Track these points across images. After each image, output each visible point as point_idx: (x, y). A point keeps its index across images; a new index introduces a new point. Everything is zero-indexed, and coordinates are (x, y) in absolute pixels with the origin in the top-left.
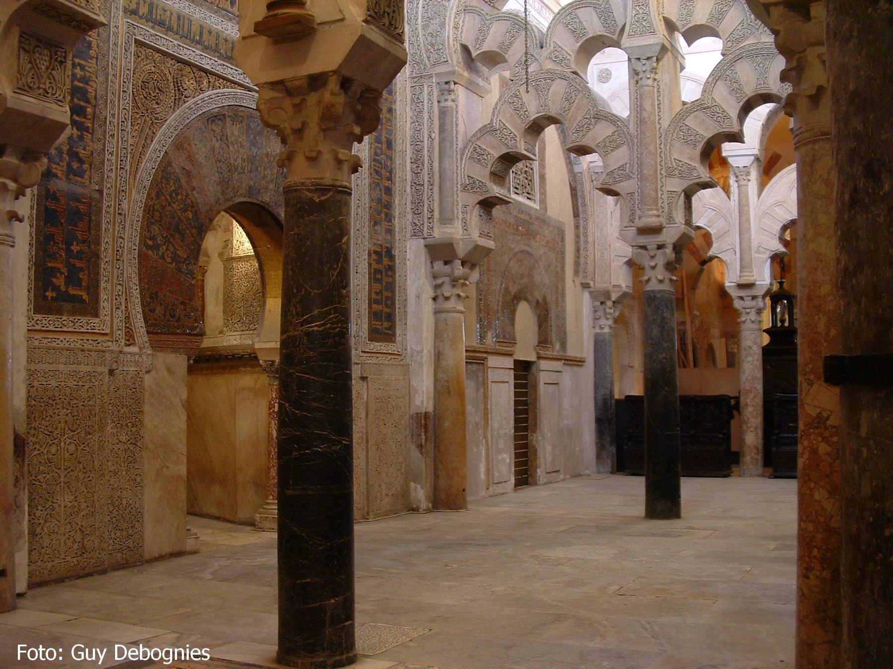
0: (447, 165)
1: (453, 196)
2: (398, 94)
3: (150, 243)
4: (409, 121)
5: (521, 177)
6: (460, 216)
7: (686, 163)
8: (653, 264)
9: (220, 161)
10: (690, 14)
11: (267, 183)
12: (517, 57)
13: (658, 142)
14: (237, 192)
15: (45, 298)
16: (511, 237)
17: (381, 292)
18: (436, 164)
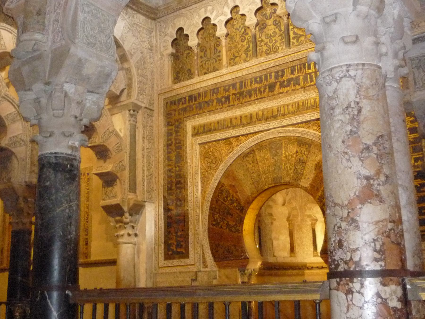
3: (214, 223)
9: (253, 173)
14: (265, 184)
15: (168, 254)
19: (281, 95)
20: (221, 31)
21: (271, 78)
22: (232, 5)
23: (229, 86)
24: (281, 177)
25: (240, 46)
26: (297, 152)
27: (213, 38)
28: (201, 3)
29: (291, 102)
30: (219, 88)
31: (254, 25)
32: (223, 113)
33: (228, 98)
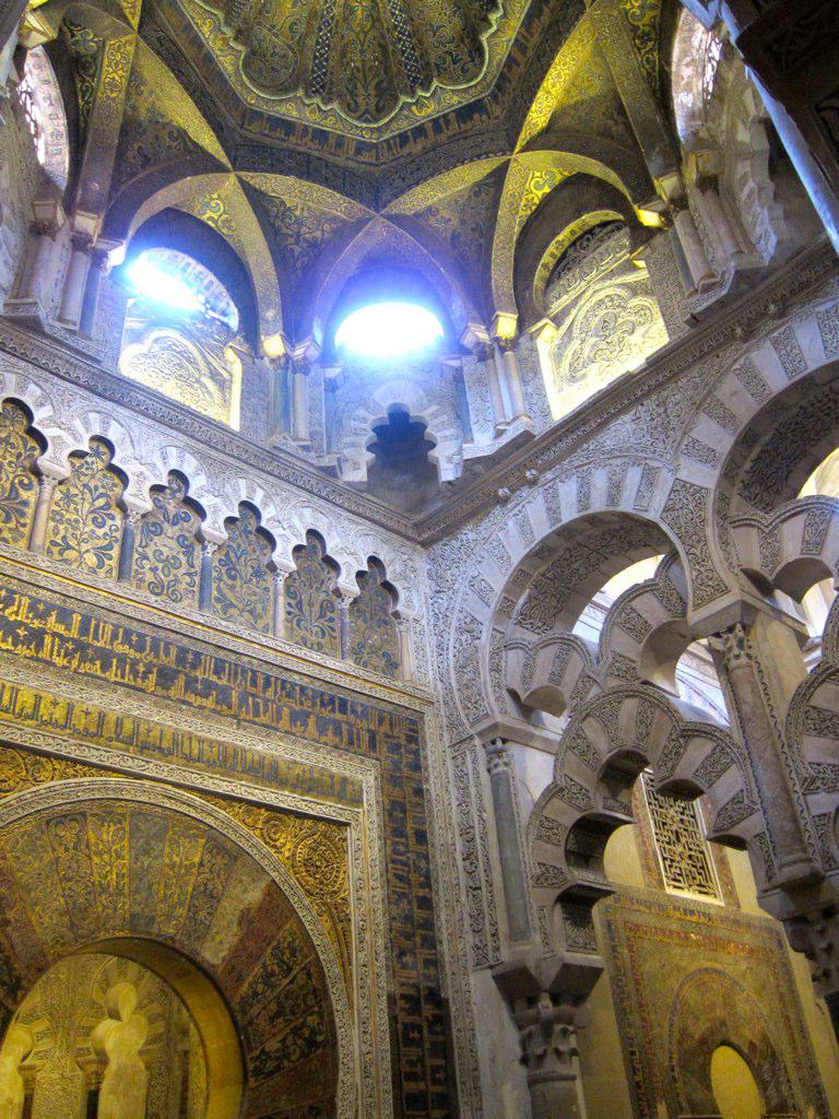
0: (508, 853)
1: (523, 897)
2: (430, 769)
4: (454, 804)
5: (683, 865)
6: (537, 924)
7: (829, 765)
8: (823, 945)
10: (776, 554)
11: (174, 907)
12: (573, 685)
13: (779, 745)
14: (104, 924)
16: (678, 951)
17: (421, 1060)
18: (494, 854)
19: (184, 707)
20: (55, 461)
21: (167, 654)
22: (97, 431)
23: (50, 607)
24: (153, 918)
25: (86, 530)
26: (201, 864)
27: (14, 460)
28: (13, 360)
29: (208, 735)
30: (13, 592)
31: (142, 512)
32: (13, 669)
33: (37, 637)
